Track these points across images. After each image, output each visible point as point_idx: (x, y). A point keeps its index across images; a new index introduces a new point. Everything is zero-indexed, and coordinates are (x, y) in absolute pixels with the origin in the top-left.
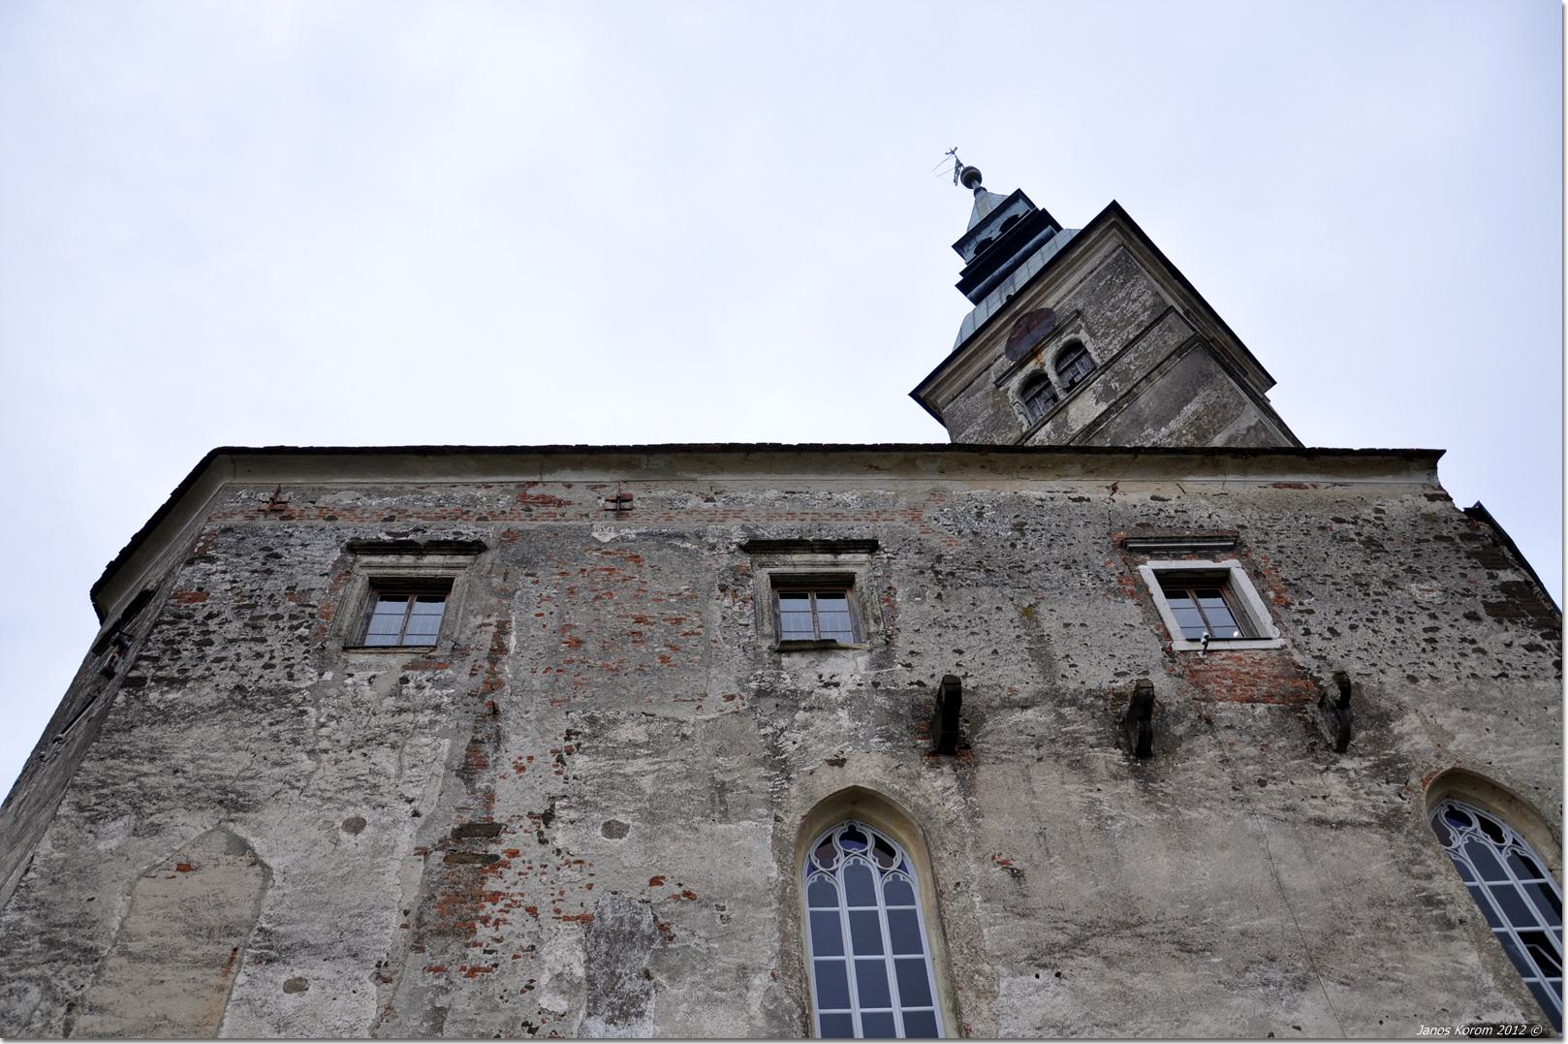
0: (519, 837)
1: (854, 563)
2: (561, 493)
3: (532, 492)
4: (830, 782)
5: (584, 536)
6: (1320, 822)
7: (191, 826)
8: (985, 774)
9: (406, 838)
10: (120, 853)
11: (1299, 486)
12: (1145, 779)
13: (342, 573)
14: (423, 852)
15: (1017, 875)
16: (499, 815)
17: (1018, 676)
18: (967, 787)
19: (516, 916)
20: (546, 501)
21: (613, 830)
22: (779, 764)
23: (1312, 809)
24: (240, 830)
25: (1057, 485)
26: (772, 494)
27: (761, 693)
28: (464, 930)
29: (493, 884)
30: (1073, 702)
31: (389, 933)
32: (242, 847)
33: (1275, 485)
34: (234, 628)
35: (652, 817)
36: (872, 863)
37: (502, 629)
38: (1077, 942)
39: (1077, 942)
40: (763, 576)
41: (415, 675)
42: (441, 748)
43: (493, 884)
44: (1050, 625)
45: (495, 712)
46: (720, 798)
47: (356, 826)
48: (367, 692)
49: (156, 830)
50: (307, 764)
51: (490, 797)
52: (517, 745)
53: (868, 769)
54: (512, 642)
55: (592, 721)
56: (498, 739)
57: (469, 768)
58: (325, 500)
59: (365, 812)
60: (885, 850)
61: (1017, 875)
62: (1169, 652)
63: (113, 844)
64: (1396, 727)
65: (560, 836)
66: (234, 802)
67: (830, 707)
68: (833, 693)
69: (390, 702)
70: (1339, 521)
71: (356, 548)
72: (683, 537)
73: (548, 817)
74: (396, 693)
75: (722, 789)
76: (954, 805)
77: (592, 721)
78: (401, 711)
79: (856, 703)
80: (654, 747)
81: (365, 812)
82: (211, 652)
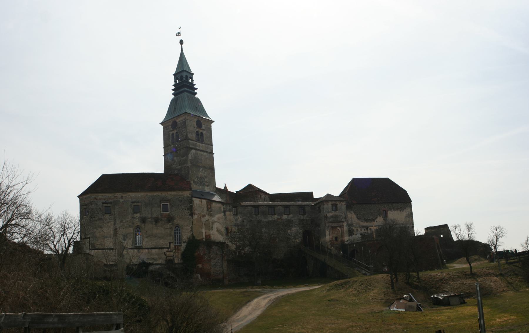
0: (118, 229)
1: (140, 204)
2: (117, 196)
3: (115, 195)
4: (136, 225)
5: (119, 201)
6: (166, 228)
7: (99, 229)
8: (146, 224)
9: (112, 230)
10: (96, 231)
11: (178, 193)
12: (156, 225)
13: (102, 206)
14: (113, 231)
15: (147, 232)
16: (117, 228)
17: (150, 216)
18: (145, 225)
19: (119, 235)
20: (116, 197)
21: (124, 229)
22: (133, 223)
23: (166, 227)
24: (102, 230)
25: (157, 193)
26: (134, 195)
27: (132, 217)
28: (116, 236)
29: (117, 233)
30: (153, 218)
31: (112, 236)
32: (103, 231)
33: (176, 193)
34: (96, 212)
35: (126, 228)
36: (139, 229)
37: (115, 212)
38: (149, 236)
39: (149, 236)
40: (133, 205)
41: (110, 217)
42: (113, 223)
43: (117, 233)
44: (153, 211)
45: (116, 220)
46: (130, 226)
47: (109, 229)
48: (107, 218)
49: (97, 230)
50: (105, 224)
51: (116, 226)
52: (117, 222)
53: (139, 224)
54: (116, 213)
55: (122, 220)
56: (116, 222)
57: (115, 224)
58: (99, 197)
59: (109, 228)
60: (140, 229)
61: (147, 232)
62: (161, 213)
63: (95, 231)
64: (175, 220)
65: (121, 229)
66: (101, 228)
67: (136, 219)
68: (137, 217)
69: (109, 219)
70: (180, 198)
71: (103, 203)
72: (127, 201)
73: (120, 228)
74: (109, 218)
75: (130, 225)
76: (143, 227)
77: (122, 220)
78: (109, 220)
79: (138, 218)
80: (125, 222)
81: (109, 228)
82: (96, 214)
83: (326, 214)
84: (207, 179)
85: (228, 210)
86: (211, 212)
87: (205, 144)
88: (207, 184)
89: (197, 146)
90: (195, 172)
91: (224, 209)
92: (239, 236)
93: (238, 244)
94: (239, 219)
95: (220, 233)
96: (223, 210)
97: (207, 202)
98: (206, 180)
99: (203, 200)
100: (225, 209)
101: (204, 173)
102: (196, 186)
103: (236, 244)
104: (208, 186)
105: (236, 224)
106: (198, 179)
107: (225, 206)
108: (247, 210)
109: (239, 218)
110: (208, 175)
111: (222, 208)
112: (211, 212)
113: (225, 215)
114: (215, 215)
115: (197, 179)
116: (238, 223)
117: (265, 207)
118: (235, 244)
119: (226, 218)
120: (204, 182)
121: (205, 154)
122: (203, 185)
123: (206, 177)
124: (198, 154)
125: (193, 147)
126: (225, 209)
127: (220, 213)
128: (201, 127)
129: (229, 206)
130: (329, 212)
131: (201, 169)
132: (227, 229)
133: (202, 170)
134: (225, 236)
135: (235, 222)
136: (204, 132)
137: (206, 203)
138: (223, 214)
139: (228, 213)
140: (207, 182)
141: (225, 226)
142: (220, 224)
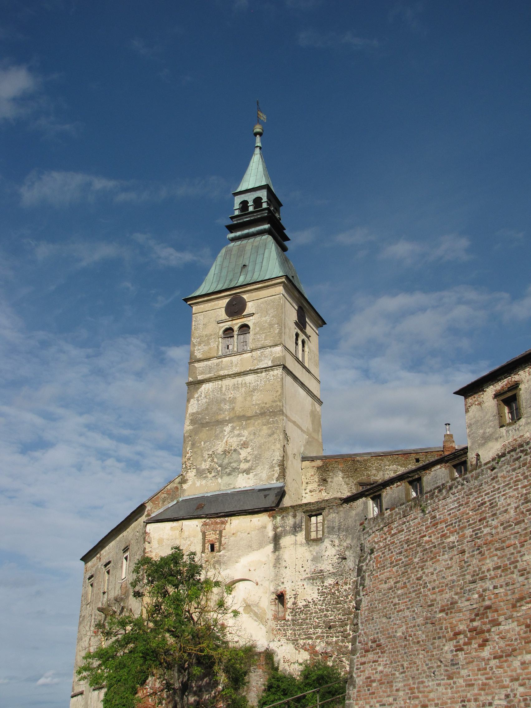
83: (478, 455)
84: (249, 450)
85: (288, 528)
86: (219, 551)
87: (252, 351)
88: (244, 466)
89: (222, 369)
90: (204, 443)
91: (275, 528)
92: (325, 615)
93: (317, 648)
94: (327, 554)
95: (256, 614)
96: (271, 534)
97: (205, 524)
98: (244, 453)
99: (185, 523)
100: (279, 530)
101: (239, 435)
102: (204, 482)
103: (313, 647)
104: (247, 471)
105: (314, 572)
106: (215, 460)
107: (279, 518)
108: (354, 512)
109: (329, 547)
110: (252, 437)
111: (270, 527)
112: (221, 553)
113: (277, 547)
114: (239, 557)
115: (212, 461)
116: (327, 566)
117: (397, 486)
118: (306, 650)
119: (278, 560)
120: (234, 465)
121: (250, 378)
122: (229, 474)
123: (245, 445)
124: (224, 389)
125: (208, 376)
126: (279, 530)
127: (261, 546)
128: (244, 310)
129: (295, 516)
130: (486, 439)
131: (228, 429)
132: (281, 598)
133: (233, 428)
134: (272, 623)
135: (310, 567)
136: (249, 321)
137: (199, 529)
138: (271, 547)
139: (286, 541)
140: (248, 459)
141: (272, 589)
142: (257, 584)
